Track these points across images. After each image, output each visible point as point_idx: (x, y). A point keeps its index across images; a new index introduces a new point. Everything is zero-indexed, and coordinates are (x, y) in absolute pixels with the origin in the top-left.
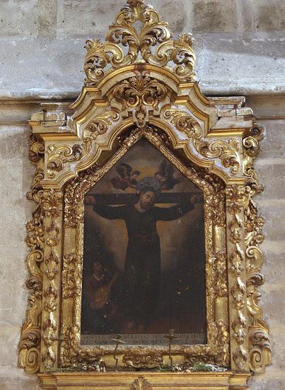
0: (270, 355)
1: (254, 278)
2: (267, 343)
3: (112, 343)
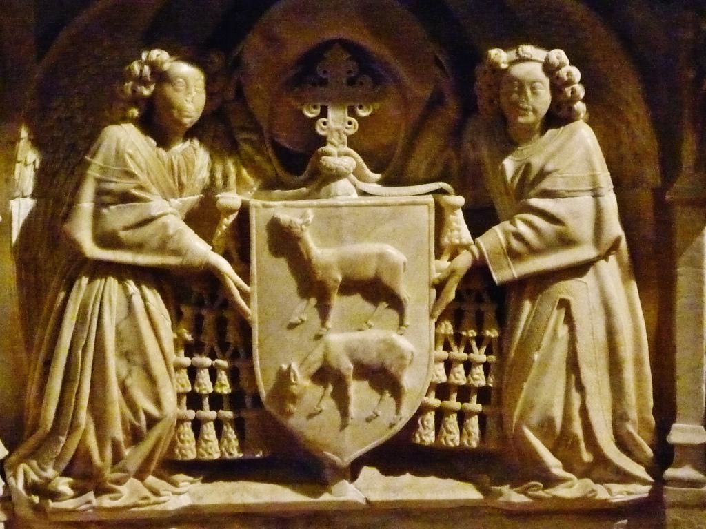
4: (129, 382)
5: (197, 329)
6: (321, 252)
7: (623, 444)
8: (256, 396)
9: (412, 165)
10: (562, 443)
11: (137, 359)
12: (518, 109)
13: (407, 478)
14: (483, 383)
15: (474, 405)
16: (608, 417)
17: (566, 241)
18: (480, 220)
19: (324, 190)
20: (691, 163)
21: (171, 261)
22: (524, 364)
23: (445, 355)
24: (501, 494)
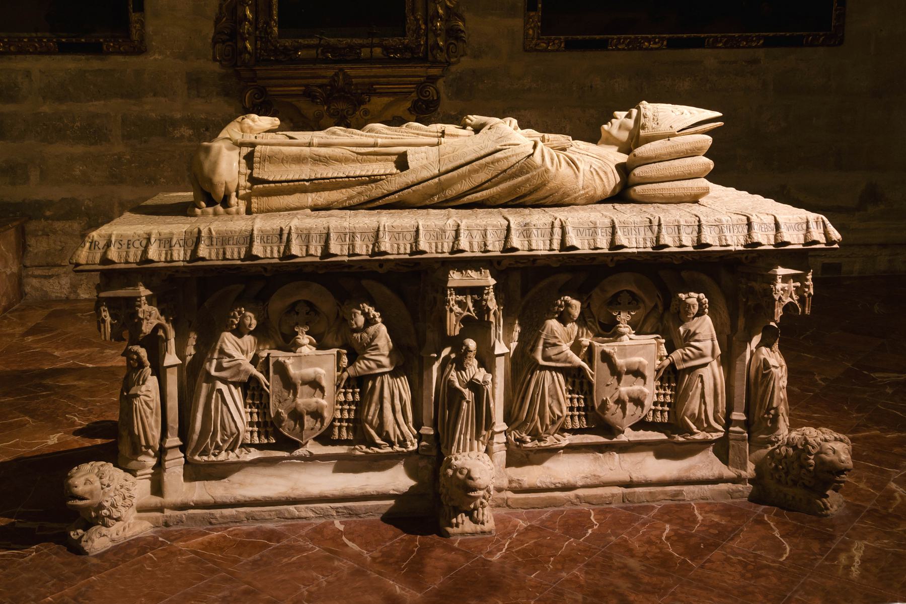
4: (552, 405)
6: (620, 361)
8: (593, 407)
9: (645, 328)
10: (697, 421)
11: (555, 397)
12: (687, 313)
13: (641, 432)
14: (670, 401)
15: (666, 408)
17: (702, 356)
18: (671, 348)
19: (619, 339)
20: (743, 327)
23: (657, 392)
24: (675, 437)
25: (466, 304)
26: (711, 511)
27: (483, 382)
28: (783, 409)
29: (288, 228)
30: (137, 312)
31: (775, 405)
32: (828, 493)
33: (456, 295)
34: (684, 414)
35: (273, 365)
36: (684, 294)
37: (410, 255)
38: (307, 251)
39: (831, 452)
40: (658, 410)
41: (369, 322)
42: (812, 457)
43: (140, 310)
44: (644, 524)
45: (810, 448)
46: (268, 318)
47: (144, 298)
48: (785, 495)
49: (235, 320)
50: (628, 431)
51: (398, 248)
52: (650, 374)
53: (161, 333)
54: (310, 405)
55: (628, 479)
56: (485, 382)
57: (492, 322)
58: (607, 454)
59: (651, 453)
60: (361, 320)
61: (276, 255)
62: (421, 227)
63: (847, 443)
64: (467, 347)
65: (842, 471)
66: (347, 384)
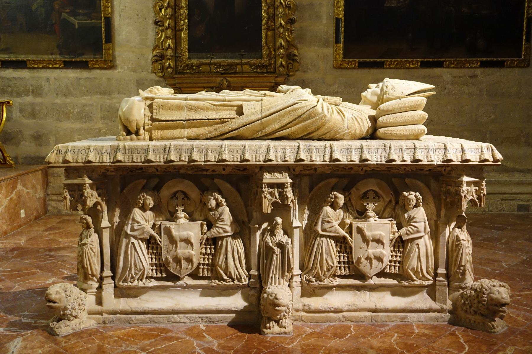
0: (298, 65)
1: (291, 19)
2: (297, 58)
3: (207, 58)
5: (341, 248)
6: (368, 233)
7: (428, 273)
8: (353, 262)
10: (416, 273)
11: (329, 254)
12: (409, 205)
13: (383, 279)
15: (397, 264)
16: (425, 267)
17: (418, 232)
18: (399, 227)
20: (443, 215)
21: (337, 235)
22: (409, 256)
23: (391, 254)
24: (402, 283)
25: (274, 193)
26: (424, 328)
27: (287, 243)
28: (469, 267)
29: (169, 145)
30: (84, 192)
31: (463, 264)
32: (496, 319)
33: (268, 188)
34: (408, 268)
35: (163, 229)
36: (407, 192)
37: (240, 162)
38: (180, 158)
39: (497, 293)
40: (392, 266)
41: (218, 205)
42: (485, 296)
43: (85, 191)
44: (382, 333)
45: (484, 290)
46: (161, 201)
47: (88, 185)
48: (470, 320)
49: (140, 201)
50: (374, 277)
51: (233, 158)
52: (387, 242)
53: (99, 207)
54: (185, 254)
55: (374, 307)
56: (287, 243)
57: (291, 207)
58: (362, 292)
59: (389, 293)
60: (213, 203)
61: (162, 160)
62: (247, 146)
63: (507, 288)
64: (277, 222)
65: (504, 305)
66: (206, 243)
